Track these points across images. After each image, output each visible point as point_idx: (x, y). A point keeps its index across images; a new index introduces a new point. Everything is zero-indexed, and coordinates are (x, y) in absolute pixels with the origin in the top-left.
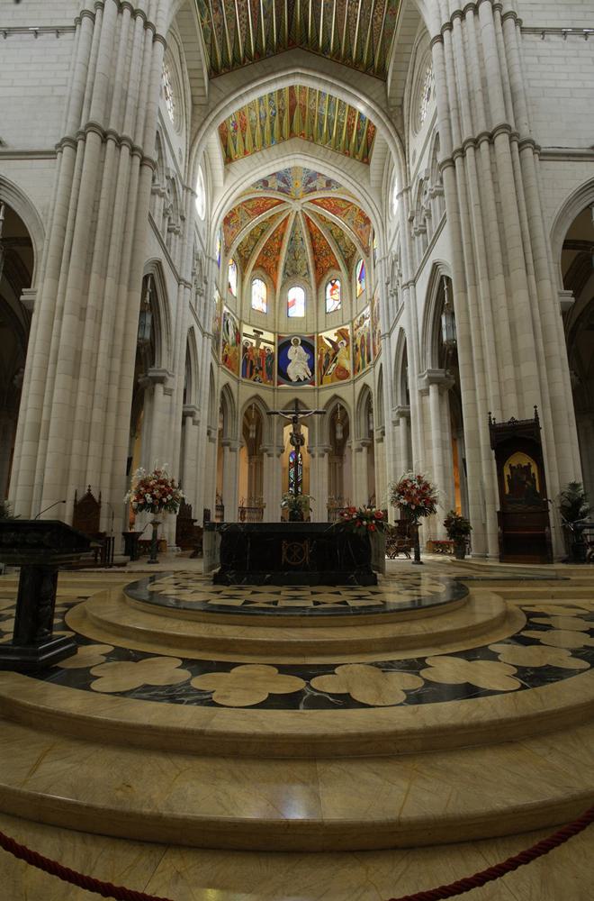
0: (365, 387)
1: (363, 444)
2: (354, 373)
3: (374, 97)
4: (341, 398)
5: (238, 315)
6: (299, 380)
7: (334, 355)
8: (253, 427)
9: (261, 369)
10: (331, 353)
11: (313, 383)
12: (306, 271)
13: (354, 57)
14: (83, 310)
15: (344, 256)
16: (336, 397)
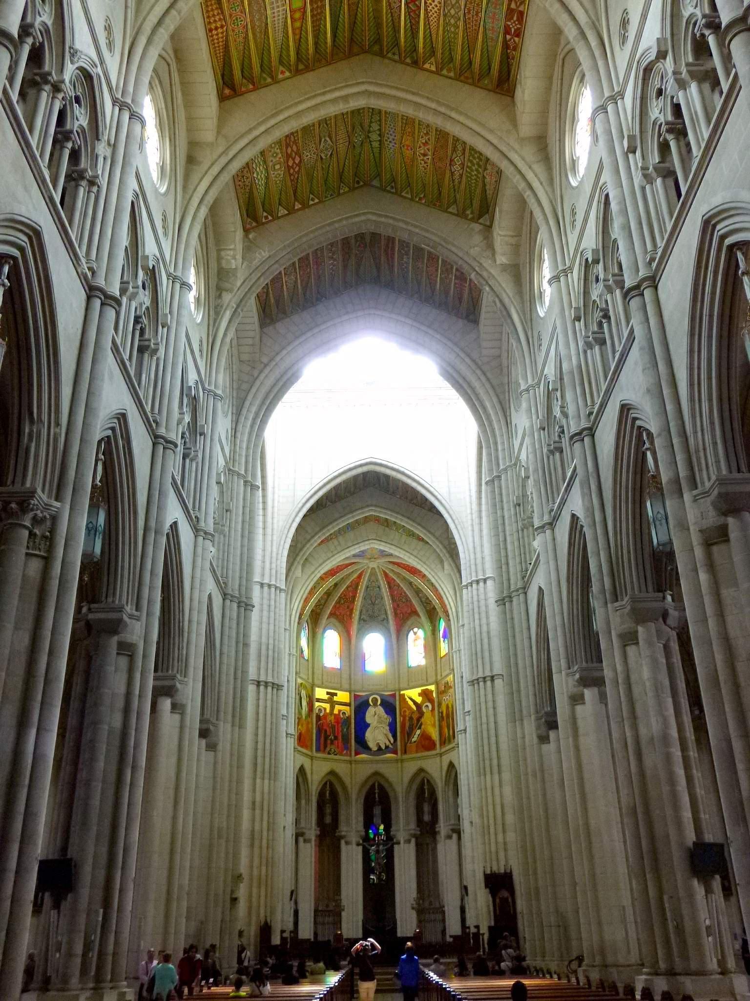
0: (451, 766)
1: (453, 831)
2: (441, 745)
3: (437, 534)
4: (427, 773)
5: (310, 680)
6: (380, 749)
7: (419, 719)
8: (328, 810)
9: (336, 738)
10: (415, 716)
11: (395, 752)
12: (384, 616)
13: (458, 62)
14: (254, 803)
15: (425, 607)
16: (421, 770)
